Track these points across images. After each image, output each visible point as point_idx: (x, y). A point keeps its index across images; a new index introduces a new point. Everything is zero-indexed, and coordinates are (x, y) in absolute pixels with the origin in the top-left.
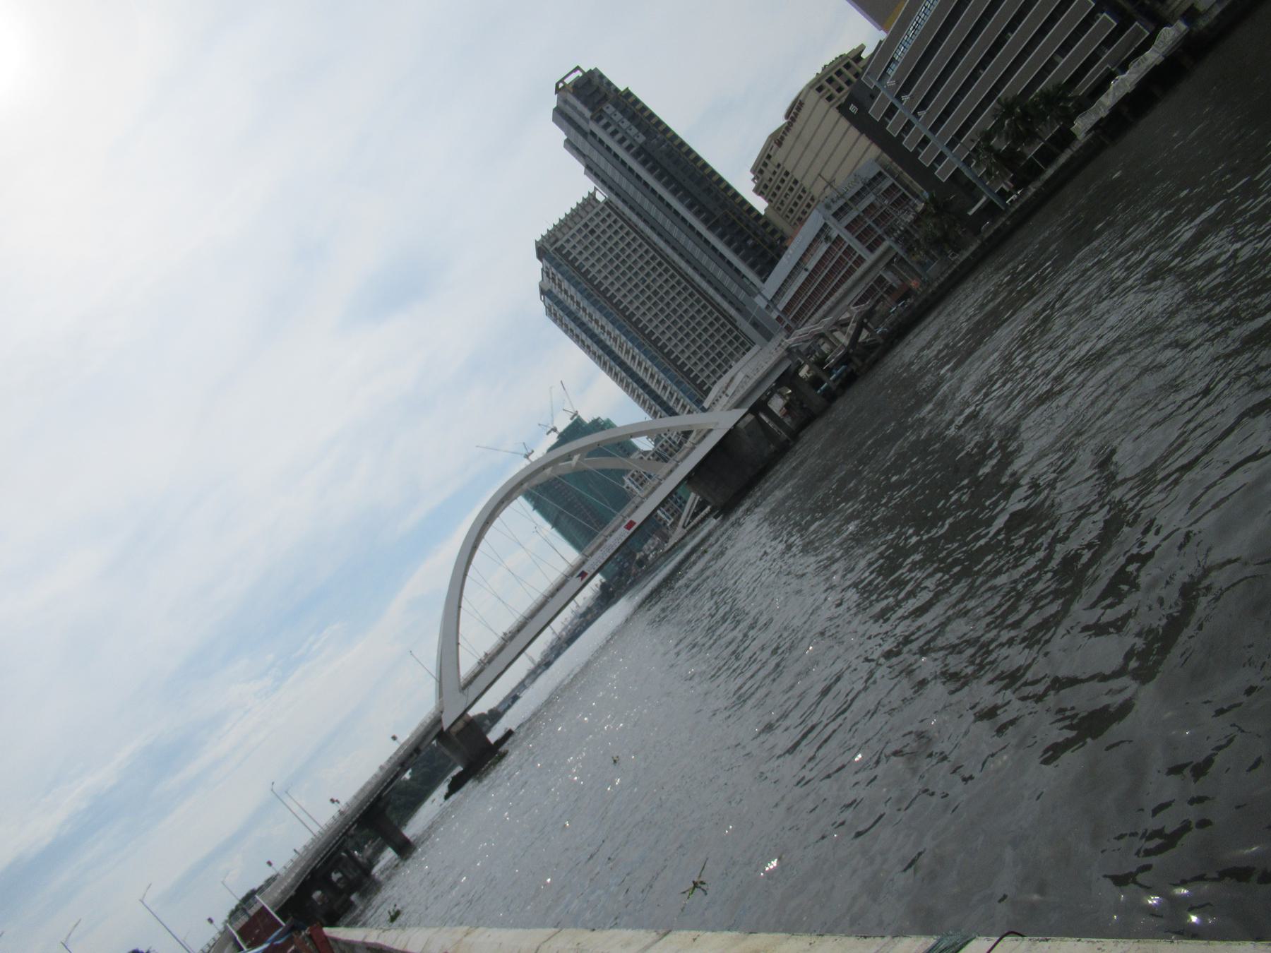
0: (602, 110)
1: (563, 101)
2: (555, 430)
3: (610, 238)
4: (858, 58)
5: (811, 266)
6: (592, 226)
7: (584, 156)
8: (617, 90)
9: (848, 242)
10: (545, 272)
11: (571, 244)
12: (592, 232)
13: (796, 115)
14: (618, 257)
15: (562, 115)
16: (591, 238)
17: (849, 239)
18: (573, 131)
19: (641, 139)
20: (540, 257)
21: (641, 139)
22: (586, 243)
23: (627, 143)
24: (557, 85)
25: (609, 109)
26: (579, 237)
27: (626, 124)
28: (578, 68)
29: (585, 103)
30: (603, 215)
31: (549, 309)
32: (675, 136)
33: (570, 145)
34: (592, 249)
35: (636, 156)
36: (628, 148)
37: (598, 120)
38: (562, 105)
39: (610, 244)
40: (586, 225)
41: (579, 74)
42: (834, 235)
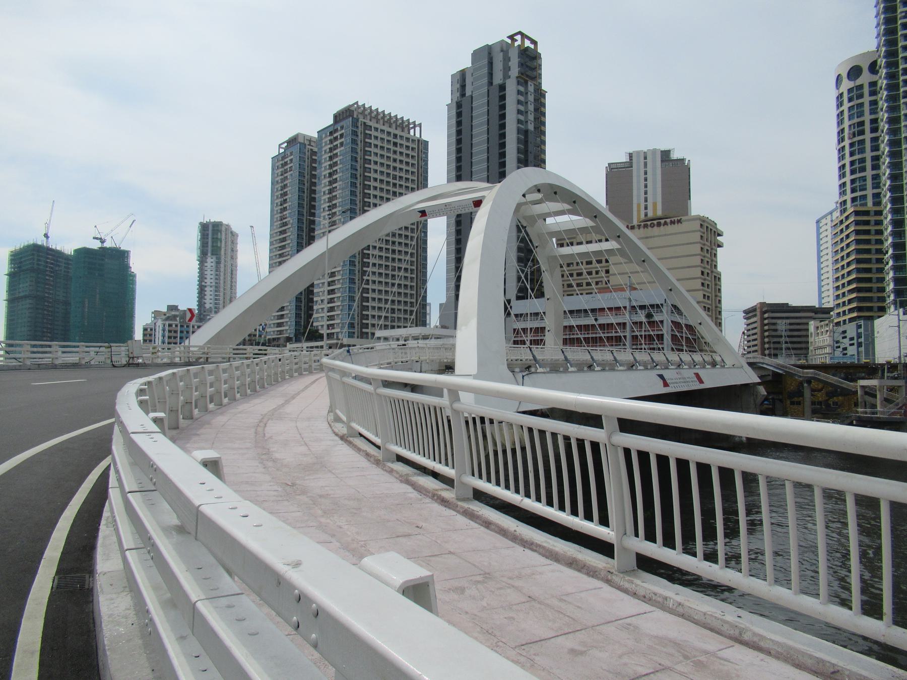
0: (526, 82)
1: (504, 48)
2: (103, 241)
3: (401, 161)
4: (719, 235)
5: (602, 320)
6: (398, 141)
7: (463, 95)
8: (540, 84)
9: (664, 332)
10: (330, 131)
11: (376, 134)
12: (395, 144)
13: (666, 223)
14: (395, 178)
15: (486, 56)
16: (391, 147)
17: (666, 331)
18: (485, 70)
19: (531, 127)
20: (339, 117)
21: (531, 127)
22: (386, 145)
23: (522, 118)
24: (520, 33)
25: (531, 88)
26: (385, 136)
27: (531, 107)
28: (534, 42)
29: (521, 65)
30: (410, 144)
31: (283, 156)
32: (544, 152)
33: (461, 80)
34: (385, 153)
35: (519, 131)
36: (519, 121)
37: (518, 83)
38: (499, 49)
39: (398, 165)
40: (395, 136)
41: (532, 46)
42: (657, 318)
